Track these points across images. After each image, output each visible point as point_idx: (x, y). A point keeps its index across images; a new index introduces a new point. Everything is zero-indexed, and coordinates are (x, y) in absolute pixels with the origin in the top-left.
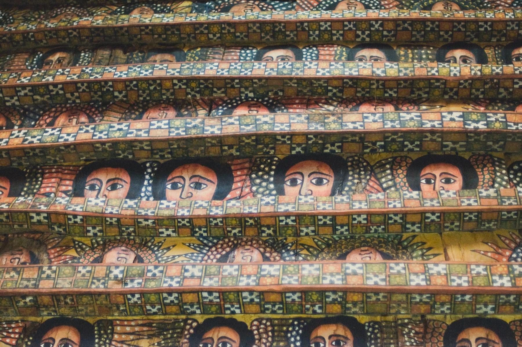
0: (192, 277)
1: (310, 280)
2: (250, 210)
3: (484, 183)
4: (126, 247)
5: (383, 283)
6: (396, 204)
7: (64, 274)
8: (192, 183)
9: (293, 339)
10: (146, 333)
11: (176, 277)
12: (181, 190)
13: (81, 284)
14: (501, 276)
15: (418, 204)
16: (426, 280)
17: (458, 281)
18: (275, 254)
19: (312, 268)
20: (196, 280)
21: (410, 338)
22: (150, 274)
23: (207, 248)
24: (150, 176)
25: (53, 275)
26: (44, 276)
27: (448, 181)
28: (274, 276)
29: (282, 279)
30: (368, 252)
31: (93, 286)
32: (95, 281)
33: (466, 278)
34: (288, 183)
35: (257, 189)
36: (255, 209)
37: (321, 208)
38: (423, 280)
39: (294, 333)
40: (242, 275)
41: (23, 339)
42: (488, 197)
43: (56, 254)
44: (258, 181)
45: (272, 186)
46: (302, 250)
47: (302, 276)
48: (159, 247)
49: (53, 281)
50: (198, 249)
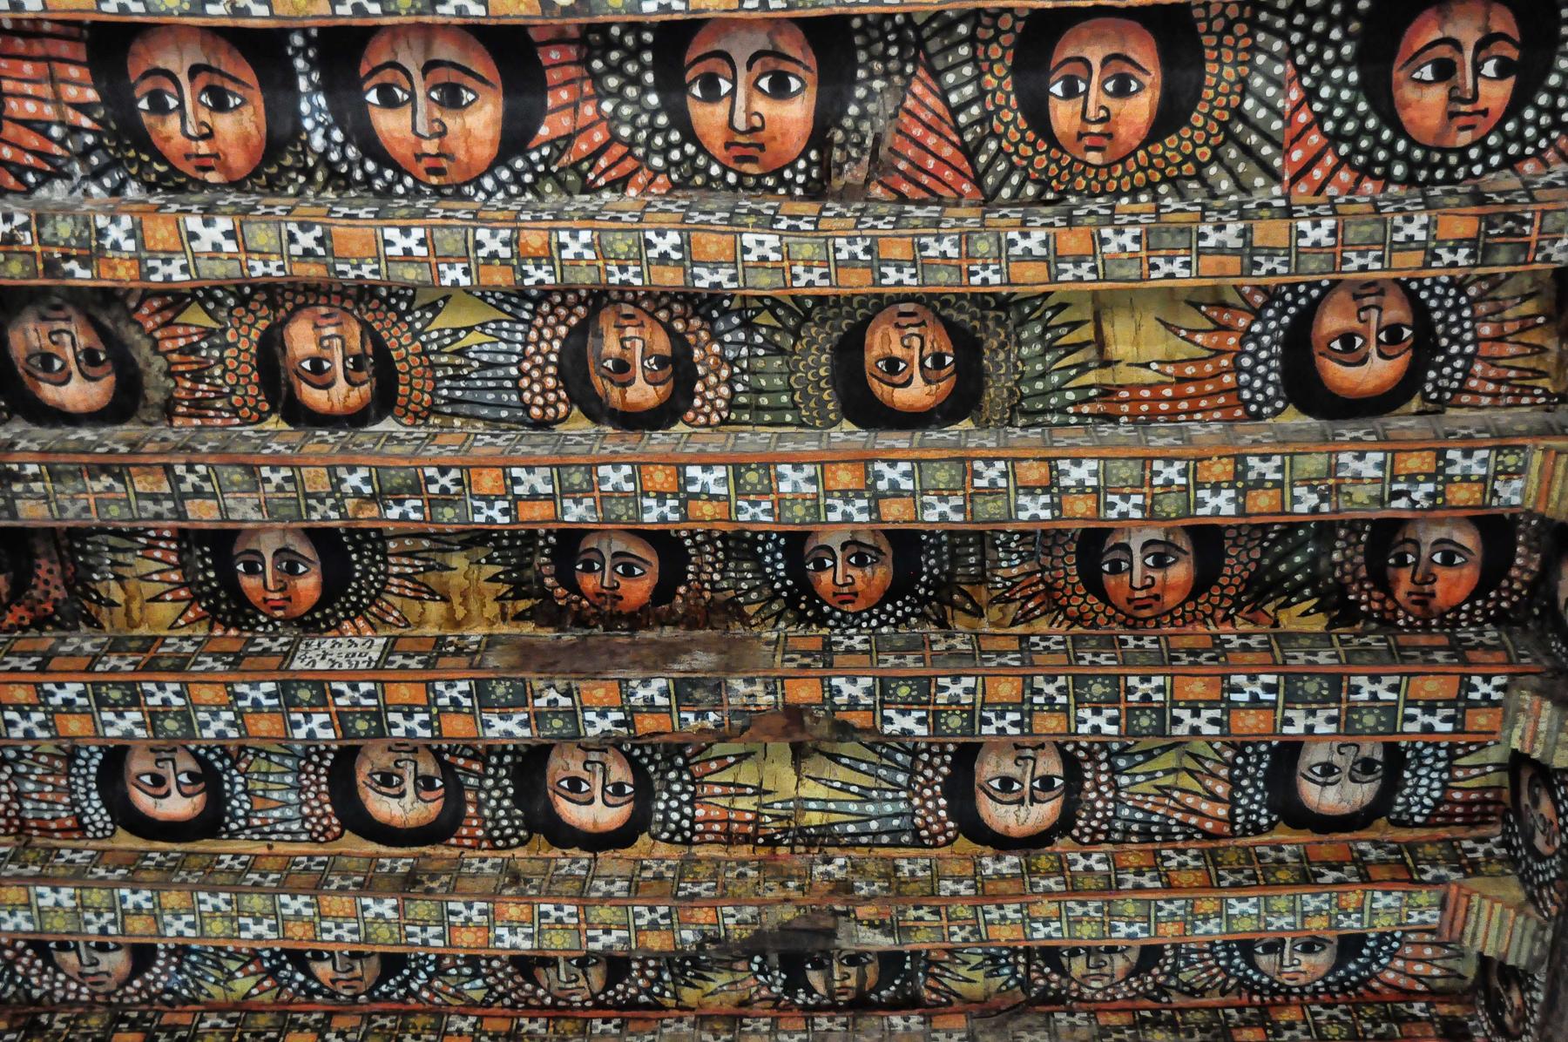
0: (534, 496)
1: (799, 510)
2: (624, 277)
3: (1217, 94)
4: (328, 305)
5: (959, 517)
6: (988, 274)
7: (233, 484)
8: (435, 88)
9: (768, 559)
10: (454, 540)
11: (498, 498)
12: (408, 109)
13: (284, 511)
14: (1216, 489)
15: (1044, 277)
16: (1050, 506)
17: (1122, 506)
18: (696, 323)
19: (799, 476)
20: (546, 504)
21: (1009, 551)
22: (434, 489)
23: (530, 306)
24: (306, 58)
25: (208, 487)
26: (186, 488)
27: (1122, 91)
28: (715, 497)
29: (739, 509)
30: (914, 320)
31: (315, 516)
32: (313, 502)
33: (1137, 499)
34: (696, 91)
35: (616, 109)
36: (636, 275)
37: (802, 283)
38: (1045, 506)
39: (769, 546)
40: (645, 494)
41: (189, 550)
42: (1220, 249)
43: (158, 319)
44: (613, 82)
45: (653, 99)
46: (759, 311)
47: (781, 500)
48: (411, 301)
49: (213, 502)
50: (508, 308)
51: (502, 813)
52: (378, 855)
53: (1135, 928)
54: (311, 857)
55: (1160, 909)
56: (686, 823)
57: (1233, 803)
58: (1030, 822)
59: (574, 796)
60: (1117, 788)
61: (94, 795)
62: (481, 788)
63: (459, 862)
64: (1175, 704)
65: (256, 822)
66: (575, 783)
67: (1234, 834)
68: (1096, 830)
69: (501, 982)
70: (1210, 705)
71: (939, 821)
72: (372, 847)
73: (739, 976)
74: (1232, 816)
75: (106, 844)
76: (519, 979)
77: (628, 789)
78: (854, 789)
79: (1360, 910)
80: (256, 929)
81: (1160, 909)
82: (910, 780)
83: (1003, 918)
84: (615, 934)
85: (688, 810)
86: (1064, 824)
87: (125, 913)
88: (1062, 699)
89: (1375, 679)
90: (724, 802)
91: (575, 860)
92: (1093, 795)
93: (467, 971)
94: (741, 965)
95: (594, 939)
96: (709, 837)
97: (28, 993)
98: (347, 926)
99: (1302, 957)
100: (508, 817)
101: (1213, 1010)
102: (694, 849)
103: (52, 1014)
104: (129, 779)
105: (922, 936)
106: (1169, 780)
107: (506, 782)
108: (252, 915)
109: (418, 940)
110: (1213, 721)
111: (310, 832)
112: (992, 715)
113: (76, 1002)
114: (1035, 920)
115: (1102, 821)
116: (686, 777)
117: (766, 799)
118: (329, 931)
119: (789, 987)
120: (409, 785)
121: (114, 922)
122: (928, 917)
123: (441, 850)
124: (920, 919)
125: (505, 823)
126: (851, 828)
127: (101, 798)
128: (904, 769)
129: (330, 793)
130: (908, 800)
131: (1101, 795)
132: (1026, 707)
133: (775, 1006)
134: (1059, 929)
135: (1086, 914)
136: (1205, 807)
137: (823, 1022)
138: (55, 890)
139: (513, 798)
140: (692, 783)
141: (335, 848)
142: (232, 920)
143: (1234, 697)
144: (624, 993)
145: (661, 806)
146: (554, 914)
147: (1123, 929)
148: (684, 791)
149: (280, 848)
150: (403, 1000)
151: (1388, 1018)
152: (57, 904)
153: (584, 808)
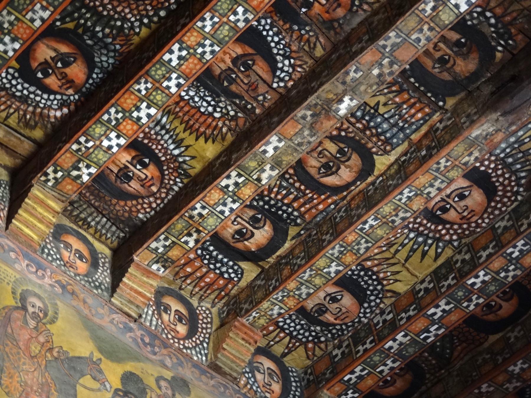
60: (411, 230)
64: (456, 307)
70: (441, 317)
79: (281, 301)
83: (432, 186)
88: (503, 275)
89: (392, 369)
99: (238, 227)
106: (392, 250)
110: (435, 314)
112: (525, 248)
114: (416, 195)
122: (467, 159)
124: (470, 155)
128: (512, 164)
130: (497, 156)
132: (514, 261)
134: (400, 200)
135: (397, 215)
143: (436, 326)
147: (371, 222)
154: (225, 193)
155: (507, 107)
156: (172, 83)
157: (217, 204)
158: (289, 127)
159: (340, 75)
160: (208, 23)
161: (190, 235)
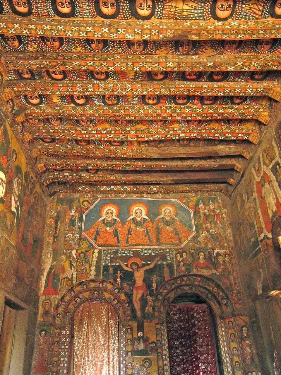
51: (127, 12)
52: (104, 21)
53: (241, 36)
54: (91, 21)
55: (247, 32)
56: (161, 14)
57: (263, 11)
58: (225, 15)
59: (140, 8)
60: (242, 7)
61: (51, 8)
62: (123, 6)
63: (118, 23)
65: (81, 13)
66: (141, 5)
67: (261, 19)
68: (237, 17)
69: (124, 49)
71: (208, 14)
72: (103, 19)
73: (167, 48)
74: (262, 14)
75: (53, 18)
76: (128, 48)
77: (151, 6)
78: (193, 7)
80: (83, 34)
81: (247, 32)
82: (204, 5)
83: (219, 33)
84: (148, 36)
85: (162, 11)
86: (231, 16)
87: (59, 31)
90: (168, 10)
91: (140, 22)
92: (237, 9)
93: (119, 46)
94: (168, 46)
95: (144, 37)
96: (165, 18)
97: (42, 50)
98: (99, 34)
99: (265, 46)
100: (128, 13)
101: (248, 56)
102: (162, 20)
103: (47, 54)
104: (57, 4)
105: (203, 37)
106: (252, 6)
107: (128, 4)
108: (82, 32)
109: (112, 37)
111: (91, 16)
113: (50, 52)
114: (224, 34)
115: (238, 15)
116: (162, 4)
117: (177, 9)
118: (96, 35)
119: (176, 50)
120: (109, 5)
121: (57, 33)
122: (205, 33)
123: (115, 20)
124: (204, 33)
125: (127, 14)
126: (192, 16)
127: (52, 8)
129: (95, 7)
130: (203, 10)
131: (239, 9)
133: (173, 55)
136: (257, 12)
137: (181, 57)
138: (47, 26)
139: (129, 8)
140: (163, 5)
141: (96, 19)
142: (79, 32)
144: (146, 51)
145: (157, 10)
146: (137, 31)
147: (239, 36)
148: (161, 7)
149: (86, 19)
150: (107, 52)
151: (277, 57)
152: (47, 29)
153: (142, 11)
154: (250, 67)
155: (185, 38)
156: (228, 91)
157: (255, 66)
158: (224, 69)
159: (204, 71)
160: (210, 94)
161: (268, 65)
